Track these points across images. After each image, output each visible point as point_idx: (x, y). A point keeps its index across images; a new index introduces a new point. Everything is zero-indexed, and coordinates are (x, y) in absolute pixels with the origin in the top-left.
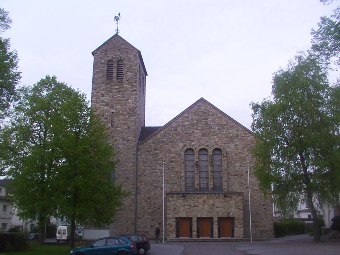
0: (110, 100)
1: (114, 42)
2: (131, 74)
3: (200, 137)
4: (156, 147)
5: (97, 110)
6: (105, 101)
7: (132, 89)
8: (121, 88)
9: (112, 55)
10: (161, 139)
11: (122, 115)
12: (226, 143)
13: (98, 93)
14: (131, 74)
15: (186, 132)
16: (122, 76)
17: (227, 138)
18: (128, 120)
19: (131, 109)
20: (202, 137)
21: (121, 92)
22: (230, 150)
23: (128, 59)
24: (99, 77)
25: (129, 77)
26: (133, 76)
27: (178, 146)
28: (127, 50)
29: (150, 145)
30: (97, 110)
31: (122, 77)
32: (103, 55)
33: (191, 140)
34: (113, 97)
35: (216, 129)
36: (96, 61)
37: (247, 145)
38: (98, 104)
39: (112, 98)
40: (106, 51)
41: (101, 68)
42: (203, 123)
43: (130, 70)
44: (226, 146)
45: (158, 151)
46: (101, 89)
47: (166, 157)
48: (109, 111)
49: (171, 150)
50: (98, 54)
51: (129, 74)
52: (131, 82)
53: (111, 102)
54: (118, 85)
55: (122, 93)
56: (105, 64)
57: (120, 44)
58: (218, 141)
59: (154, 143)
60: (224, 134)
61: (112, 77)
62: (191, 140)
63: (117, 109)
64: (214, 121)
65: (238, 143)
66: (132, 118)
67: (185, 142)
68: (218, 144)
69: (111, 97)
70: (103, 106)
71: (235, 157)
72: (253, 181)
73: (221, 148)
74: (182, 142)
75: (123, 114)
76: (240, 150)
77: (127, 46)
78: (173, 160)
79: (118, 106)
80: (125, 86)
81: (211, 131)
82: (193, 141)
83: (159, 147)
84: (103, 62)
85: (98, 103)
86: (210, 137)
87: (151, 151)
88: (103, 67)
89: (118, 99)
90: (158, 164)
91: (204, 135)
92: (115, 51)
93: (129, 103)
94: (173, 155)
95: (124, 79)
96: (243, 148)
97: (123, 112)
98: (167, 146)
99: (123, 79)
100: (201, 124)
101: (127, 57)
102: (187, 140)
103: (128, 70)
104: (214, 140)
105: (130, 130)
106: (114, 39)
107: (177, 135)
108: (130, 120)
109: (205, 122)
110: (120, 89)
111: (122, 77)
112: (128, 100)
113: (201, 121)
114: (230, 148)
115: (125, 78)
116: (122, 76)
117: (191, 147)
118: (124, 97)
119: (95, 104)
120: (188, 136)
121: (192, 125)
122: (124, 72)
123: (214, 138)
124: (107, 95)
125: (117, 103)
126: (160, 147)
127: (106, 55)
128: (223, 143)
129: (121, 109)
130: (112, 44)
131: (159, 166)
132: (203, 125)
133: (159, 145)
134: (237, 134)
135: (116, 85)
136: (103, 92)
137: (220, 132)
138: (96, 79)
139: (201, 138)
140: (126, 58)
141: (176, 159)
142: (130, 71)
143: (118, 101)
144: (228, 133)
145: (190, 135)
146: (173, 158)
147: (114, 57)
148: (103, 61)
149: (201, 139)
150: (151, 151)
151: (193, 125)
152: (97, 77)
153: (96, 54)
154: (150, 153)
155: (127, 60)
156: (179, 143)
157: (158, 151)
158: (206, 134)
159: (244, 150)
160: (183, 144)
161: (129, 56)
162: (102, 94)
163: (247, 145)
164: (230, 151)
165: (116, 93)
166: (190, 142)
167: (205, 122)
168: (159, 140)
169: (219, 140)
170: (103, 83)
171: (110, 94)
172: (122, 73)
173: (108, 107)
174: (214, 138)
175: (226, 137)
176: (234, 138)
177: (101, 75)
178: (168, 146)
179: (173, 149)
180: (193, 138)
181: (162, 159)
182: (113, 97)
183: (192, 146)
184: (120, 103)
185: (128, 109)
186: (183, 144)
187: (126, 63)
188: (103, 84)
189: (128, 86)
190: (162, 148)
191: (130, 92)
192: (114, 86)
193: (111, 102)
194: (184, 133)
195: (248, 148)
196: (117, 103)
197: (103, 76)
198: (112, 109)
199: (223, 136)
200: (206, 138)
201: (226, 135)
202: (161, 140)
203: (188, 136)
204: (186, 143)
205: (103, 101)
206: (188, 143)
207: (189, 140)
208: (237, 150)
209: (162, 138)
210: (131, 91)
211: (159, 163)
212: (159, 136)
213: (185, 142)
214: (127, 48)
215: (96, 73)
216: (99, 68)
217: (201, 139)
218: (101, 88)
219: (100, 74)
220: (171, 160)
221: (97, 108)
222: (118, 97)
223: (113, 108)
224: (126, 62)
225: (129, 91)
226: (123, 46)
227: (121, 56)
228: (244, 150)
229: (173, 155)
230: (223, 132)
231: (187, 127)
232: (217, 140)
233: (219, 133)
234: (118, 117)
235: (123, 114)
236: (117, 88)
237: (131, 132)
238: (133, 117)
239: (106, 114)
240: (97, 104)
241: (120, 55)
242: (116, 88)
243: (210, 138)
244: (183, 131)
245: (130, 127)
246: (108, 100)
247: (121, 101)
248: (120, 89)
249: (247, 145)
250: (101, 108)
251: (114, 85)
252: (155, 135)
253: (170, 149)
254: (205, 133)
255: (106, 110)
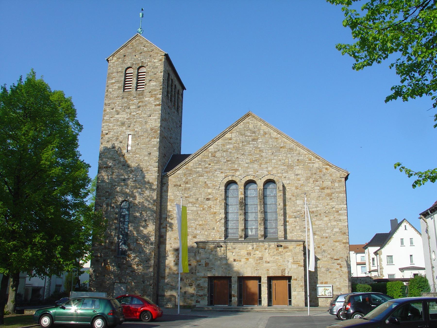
0: (127, 119)
1: (134, 44)
2: (154, 83)
3: (247, 165)
4: (187, 180)
5: (110, 132)
6: (120, 119)
7: (155, 103)
8: (142, 102)
9: (132, 61)
10: (195, 168)
11: (141, 137)
12: (283, 172)
13: (112, 110)
14: (154, 83)
15: (228, 159)
16: (143, 86)
17: (284, 166)
18: (149, 144)
19: (153, 130)
20: (250, 165)
21: (141, 108)
22: (288, 182)
23: (152, 64)
24: (113, 90)
25: (151, 88)
26: (157, 86)
27: (218, 177)
28: (151, 53)
29: (179, 177)
30: (110, 132)
31: (143, 88)
32: (120, 61)
33: (234, 170)
34: (130, 114)
35: (270, 154)
36: (112, 69)
37: (312, 174)
38: (112, 124)
39: (129, 116)
40: (125, 56)
41: (117, 78)
42: (251, 146)
43: (153, 78)
44: (283, 177)
45: (190, 186)
46: (116, 104)
47: (201, 193)
48: (125, 133)
49: (207, 184)
50: (113, 61)
51: (152, 84)
52: (155, 94)
53: (127, 121)
54: (138, 98)
55: (142, 109)
56: (122, 72)
57: (143, 46)
58: (271, 171)
59: (185, 175)
60: (280, 161)
61: (130, 89)
62: (234, 170)
63: (135, 130)
64: (266, 143)
65: (299, 172)
66: (154, 141)
67: (227, 173)
68: (272, 174)
69: (129, 114)
70: (118, 127)
71: (296, 191)
72: (321, 225)
73: (275, 179)
74: (222, 173)
75: (142, 136)
76: (303, 182)
77: (151, 48)
78: (210, 197)
79: (137, 126)
80: (147, 99)
81: (262, 156)
82: (236, 170)
83: (191, 180)
84: (120, 70)
85: (111, 123)
86: (261, 164)
87: (180, 186)
88: (121, 76)
89: (136, 117)
90: (189, 202)
91: (252, 162)
92: (135, 56)
93: (151, 121)
94: (209, 191)
95: (146, 90)
96: (308, 179)
97: (142, 134)
98: (201, 179)
99: (145, 91)
100: (248, 148)
101: (151, 62)
102: (229, 170)
103: (151, 78)
104: (266, 169)
105: (151, 158)
106: (135, 41)
107: (216, 163)
108: (151, 144)
109: (253, 144)
110: (140, 104)
111: (143, 88)
112: (150, 118)
113: (249, 144)
114: (289, 179)
115: (147, 89)
116: (143, 86)
117: (234, 179)
118: (145, 114)
119: (107, 124)
120: (230, 164)
121: (236, 150)
122: (146, 81)
123: (266, 166)
124: (124, 112)
125: (135, 122)
126: (193, 180)
127: (124, 61)
128: (278, 173)
129: (140, 130)
130: (132, 47)
131: (191, 206)
132: (251, 149)
133: (191, 178)
134: (298, 160)
135: (135, 98)
136: (118, 108)
137: (275, 157)
138: (111, 92)
139: (248, 166)
140: (149, 63)
141: (214, 195)
142: (153, 80)
143: (137, 119)
144: (286, 159)
145: (234, 163)
146: (210, 194)
147: (135, 63)
148: (120, 69)
149: (248, 167)
150: (180, 186)
151: (237, 149)
152: (111, 89)
153: (112, 61)
154: (179, 188)
155: (150, 66)
156: (217, 174)
157: (190, 186)
158: (255, 161)
159: (308, 181)
160: (223, 175)
161: (153, 61)
162: (117, 111)
163: (312, 174)
164: (289, 183)
165: (134, 109)
166: (233, 172)
167: (253, 144)
168: (191, 170)
169: (273, 168)
170: (119, 97)
171: (128, 111)
172: (144, 83)
173: (124, 128)
174: (266, 166)
175: (284, 164)
176: (294, 165)
177: (117, 87)
178: (202, 178)
179: (210, 182)
180: (238, 167)
181: (195, 197)
182: (130, 114)
183: (234, 177)
184: (139, 122)
185: (149, 129)
186: (223, 175)
187: (149, 69)
188: (118, 98)
189: (150, 100)
190: (195, 181)
191: (153, 107)
192: (132, 101)
193: (128, 122)
194: (225, 160)
195: (314, 179)
196: (135, 122)
197: (119, 88)
198: (129, 131)
199: (279, 163)
200: (256, 166)
201: (282, 161)
202: (194, 170)
203: (230, 164)
204: (228, 174)
205: (118, 120)
206: (230, 173)
207: (232, 170)
208: (298, 182)
209: (195, 167)
210: (154, 105)
211: (191, 201)
212: (191, 164)
213: (227, 173)
214: (152, 51)
215: (110, 84)
216: (114, 78)
217: (248, 167)
218: (116, 103)
219: (116, 86)
220: (207, 197)
221: (109, 129)
222: (137, 114)
223: (130, 128)
224: (149, 68)
225: (151, 106)
226: (146, 49)
227: (143, 62)
228: (308, 181)
229: (209, 191)
230: (279, 157)
231: (230, 152)
232: (270, 169)
233: (273, 159)
234: (136, 140)
235: (142, 136)
236: (136, 103)
237: (152, 159)
238: (155, 140)
239: (121, 136)
240: (110, 125)
241: (142, 61)
242: (135, 102)
243: (260, 166)
244: (224, 158)
245: (152, 154)
246: (125, 118)
247: (141, 119)
248: (140, 104)
249: (312, 175)
250: (115, 129)
251: (132, 99)
252: (186, 164)
253: (205, 182)
254: (254, 159)
255: (121, 131)
